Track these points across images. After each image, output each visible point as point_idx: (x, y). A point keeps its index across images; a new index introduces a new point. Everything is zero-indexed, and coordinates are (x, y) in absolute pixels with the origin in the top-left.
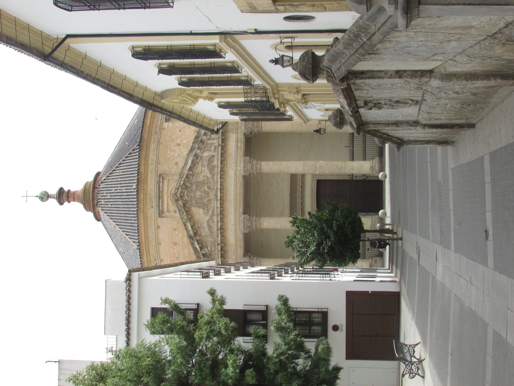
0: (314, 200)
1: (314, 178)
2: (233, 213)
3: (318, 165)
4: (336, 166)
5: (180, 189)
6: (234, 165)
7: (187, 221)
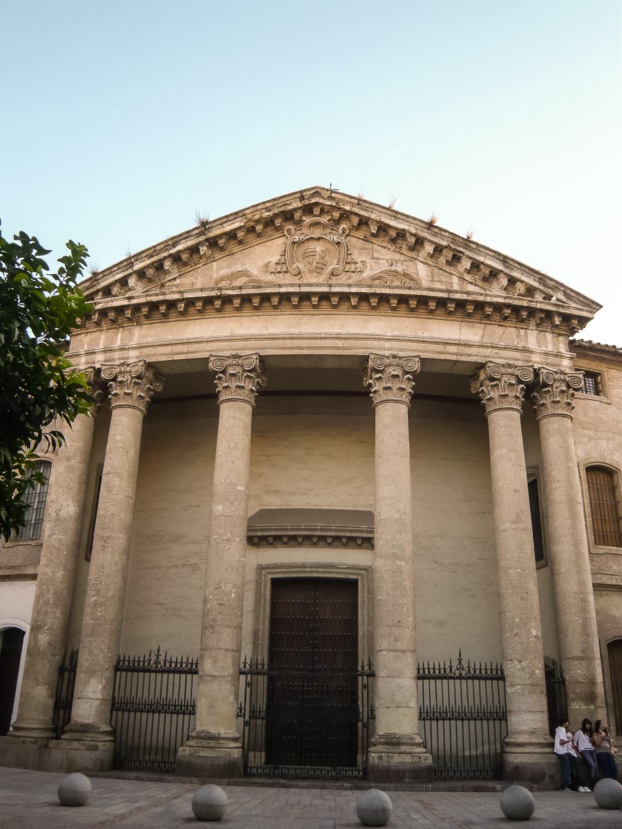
1: (362, 572)
2: (264, 332)
3: (403, 563)
4: (399, 622)
5: (329, 203)
6: (397, 333)
7: (250, 220)
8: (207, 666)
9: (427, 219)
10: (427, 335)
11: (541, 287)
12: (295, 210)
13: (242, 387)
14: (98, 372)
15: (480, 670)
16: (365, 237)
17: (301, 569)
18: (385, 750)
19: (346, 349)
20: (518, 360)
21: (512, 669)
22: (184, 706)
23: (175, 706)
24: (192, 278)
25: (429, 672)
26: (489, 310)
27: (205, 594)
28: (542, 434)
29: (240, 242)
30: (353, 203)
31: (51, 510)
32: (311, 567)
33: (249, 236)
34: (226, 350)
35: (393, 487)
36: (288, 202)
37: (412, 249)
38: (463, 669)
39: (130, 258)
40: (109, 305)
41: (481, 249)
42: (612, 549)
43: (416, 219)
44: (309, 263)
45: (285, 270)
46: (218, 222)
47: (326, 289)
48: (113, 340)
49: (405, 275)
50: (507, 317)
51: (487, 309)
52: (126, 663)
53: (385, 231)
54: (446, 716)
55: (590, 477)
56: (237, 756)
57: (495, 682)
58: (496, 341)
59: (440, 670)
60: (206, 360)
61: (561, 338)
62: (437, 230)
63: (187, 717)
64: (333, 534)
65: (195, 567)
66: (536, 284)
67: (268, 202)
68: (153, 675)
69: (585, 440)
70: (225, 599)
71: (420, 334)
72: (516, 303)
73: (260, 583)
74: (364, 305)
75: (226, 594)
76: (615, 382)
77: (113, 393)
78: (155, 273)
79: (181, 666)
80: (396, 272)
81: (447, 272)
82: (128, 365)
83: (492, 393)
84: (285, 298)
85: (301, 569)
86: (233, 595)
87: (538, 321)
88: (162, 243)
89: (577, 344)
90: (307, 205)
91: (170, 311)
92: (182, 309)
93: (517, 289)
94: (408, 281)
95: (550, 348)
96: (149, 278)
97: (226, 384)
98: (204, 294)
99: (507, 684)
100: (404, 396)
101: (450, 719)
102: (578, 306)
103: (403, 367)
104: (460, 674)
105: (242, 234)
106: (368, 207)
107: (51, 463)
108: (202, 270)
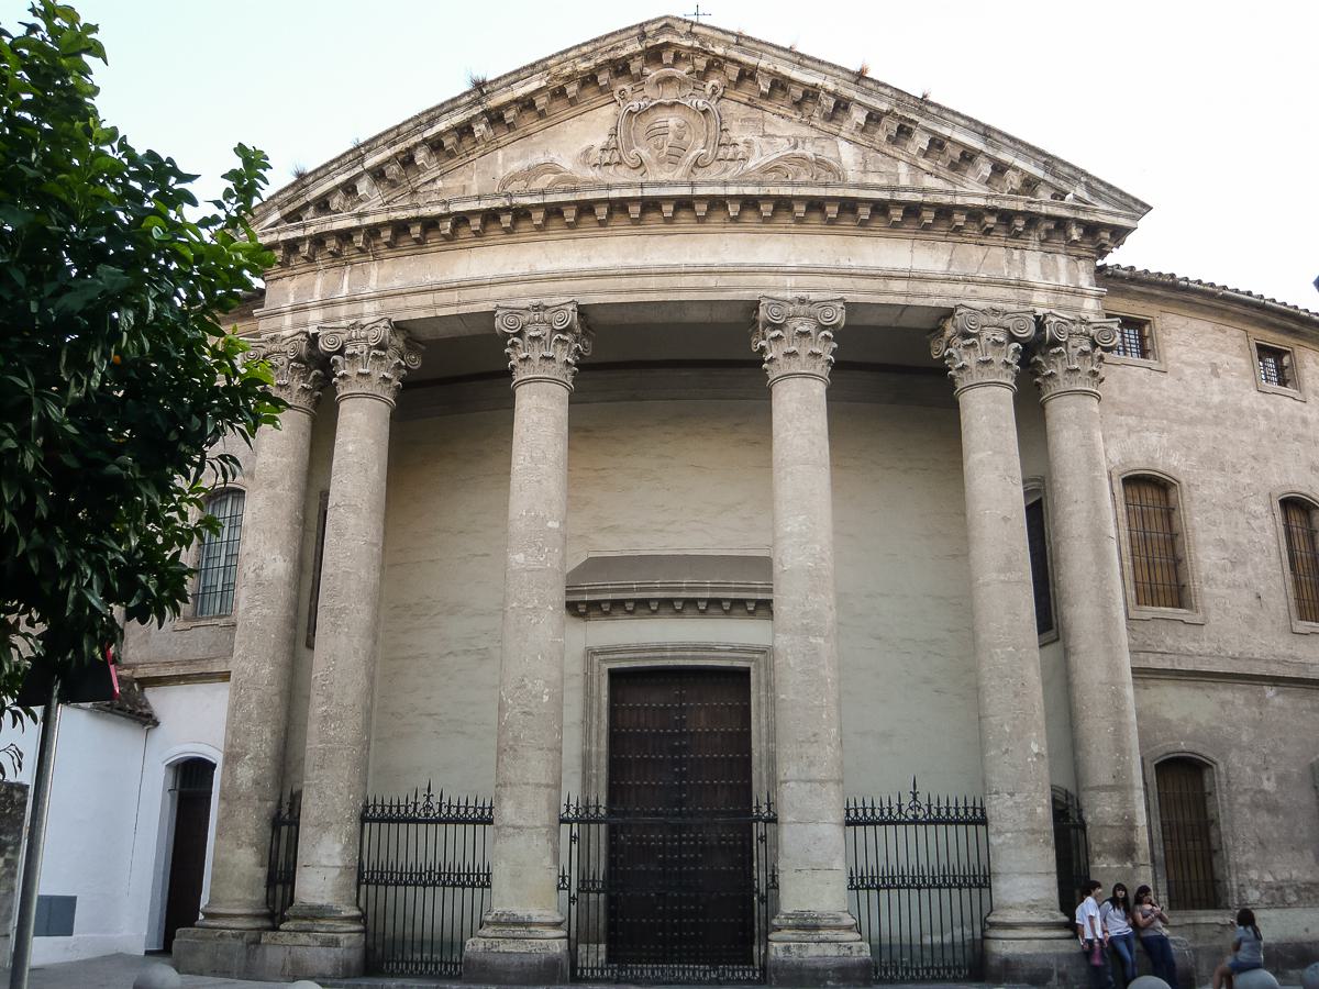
0: (663, 658)
1: (757, 656)
2: (586, 265)
6: (806, 262)
7: (555, 77)
8: (507, 812)
9: (855, 68)
10: (855, 263)
11: (1048, 178)
12: (632, 56)
13: (552, 359)
14: (313, 340)
15: (948, 809)
16: (749, 99)
17: (657, 654)
18: (795, 937)
19: (722, 290)
20: (1009, 301)
21: (999, 808)
22: (474, 874)
23: (459, 875)
24: (463, 178)
25: (865, 814)
26: (960, 219)
27: (501, 698)
28: (1049, 423)
29: (542, 115)
30: (729, 43)
31: (247, 569)
32: (673, 650)
33: (555, 104)
34: (523, 296)
35: (801, 518)
36: (621, 44)
37: (830, 117)
38: (919, 808)
39: (359, 147)
40: (327, 228)
41: (946, 115)
42: (1166, 612)
43: (835, 67)
44: (656, 147)
45: (617, 159)
46: (504, 82)
47: (686, 191)
48: (336, 287)
49: (820, 163)
50: (990, 230)
51: (956, 217)
52: (379, 810)
53: (783, 88)
54: (893, 882)
55: (1129, 493)
56: (558, 951)
57: (972, 828)
58: (971, 270)
59: (882, 810)
60: (491, 315)
61: (1082, 264)
62: (871, 85)
63: (478, 891)
64: (708, 595)
65: (483, 655)
66: (1040, 173)
67: (585, 44)
68: (422, 827)
69: (1122, 432)
70: (533, 705)
71: (844, 263)
72: (1007, 205)
73: (591, 678)
74: (750, 215)
75: (535, 696)
76: (1174, 335)
77: (339, 374)
78: (400, 171)
79: (466, 812)
80: (804, 158)
81: (889, 156)
82: (362, 327)
83: (966, 358)
84: (618, 206)
85: (657, 654)
86: (546, 698)
87: (1043, 236)
88: (409, 121)
89: (1110, 273)
90: (652, 47)
91: (428, 236)
92: (448, 232)
93: (1008, 181)
94: (824, 173)
95: (1063, 281)
96: (391, 181)
97: (524, 355)
98: (484, 205)
99: (991, 830)
100: (819, 367)
101: (899, 887)
102: (1110, 209)
103: (816, 318)
104: (916, 817)
105: (544, 100)
106: (756, 49)
107: (244, 492)
108: (479, 163)
